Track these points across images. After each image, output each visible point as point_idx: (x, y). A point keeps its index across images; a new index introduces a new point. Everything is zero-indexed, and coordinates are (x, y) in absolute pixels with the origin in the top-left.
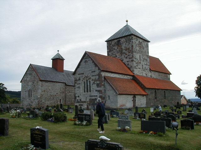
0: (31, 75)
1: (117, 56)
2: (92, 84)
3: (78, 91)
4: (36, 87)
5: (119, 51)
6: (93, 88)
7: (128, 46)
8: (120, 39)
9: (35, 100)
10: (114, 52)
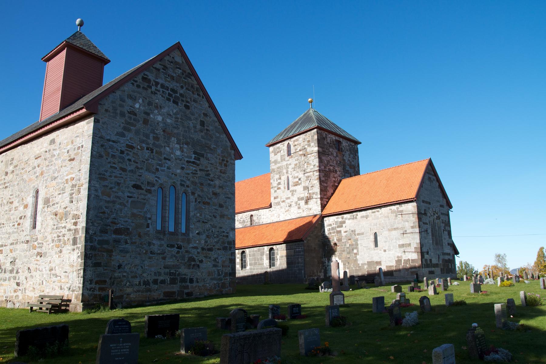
0: (181, 106)
1: (336, 172)
2: (444, 230)
3: (426, 241)
4: (217, 182)
5: (340, 162)
6: (444, 239)
7: (353, 162)
8: (341, 140)
9: (213, 254)
10: (331, 159)
